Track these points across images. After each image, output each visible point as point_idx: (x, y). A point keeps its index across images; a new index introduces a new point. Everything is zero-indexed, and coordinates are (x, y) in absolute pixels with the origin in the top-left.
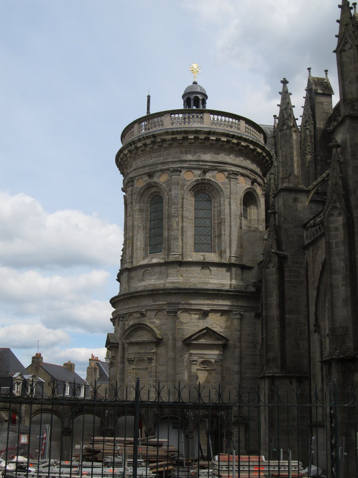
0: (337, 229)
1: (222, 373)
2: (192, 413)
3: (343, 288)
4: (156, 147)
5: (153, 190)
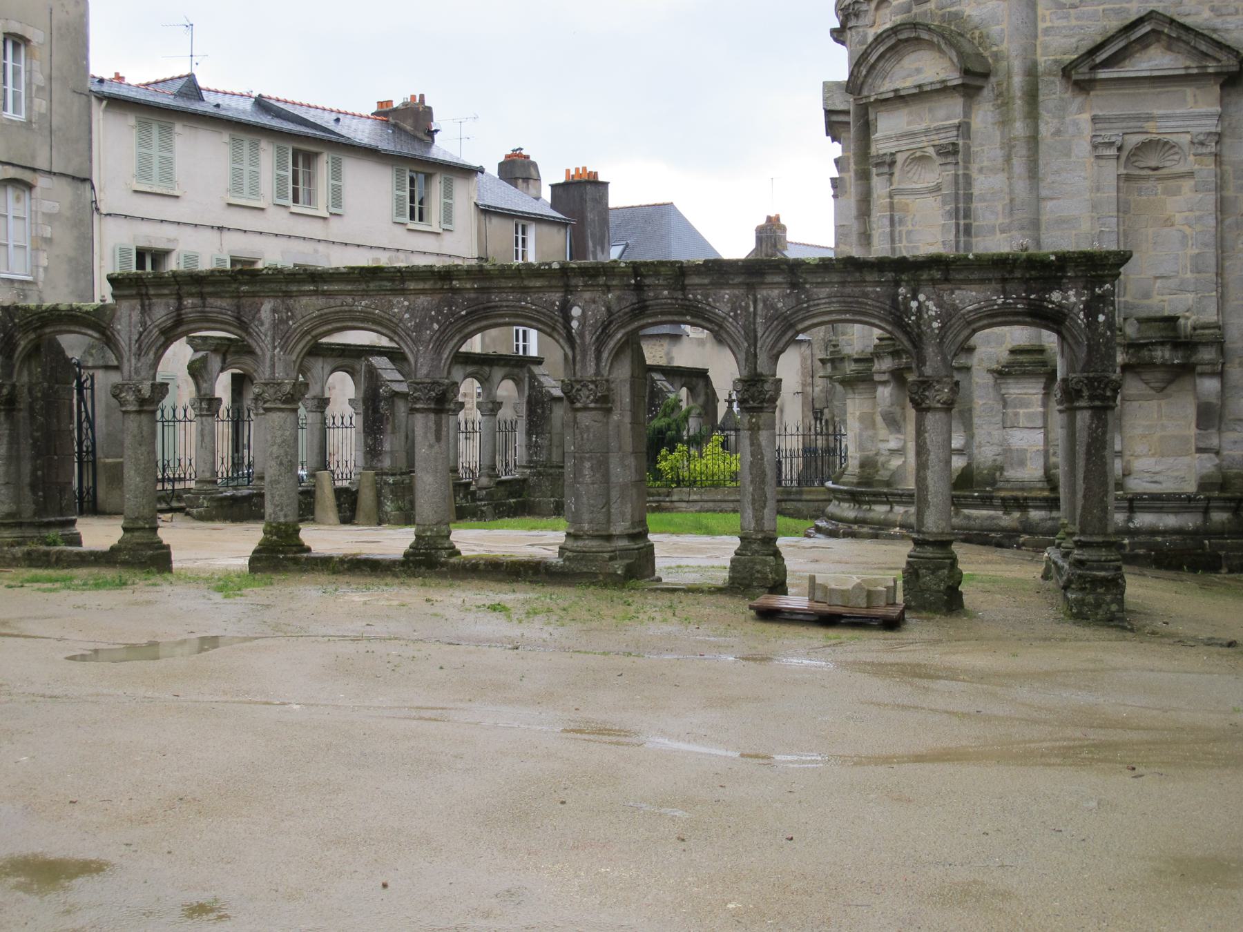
1: (1220, 187)
2: (930, 304)
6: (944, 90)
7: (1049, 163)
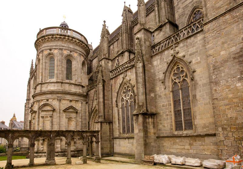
0: (139, 68)
3: (142, 89)
4: (53, 39)
5: (51, 56)
6: (51, 110)
7: (61, 119)
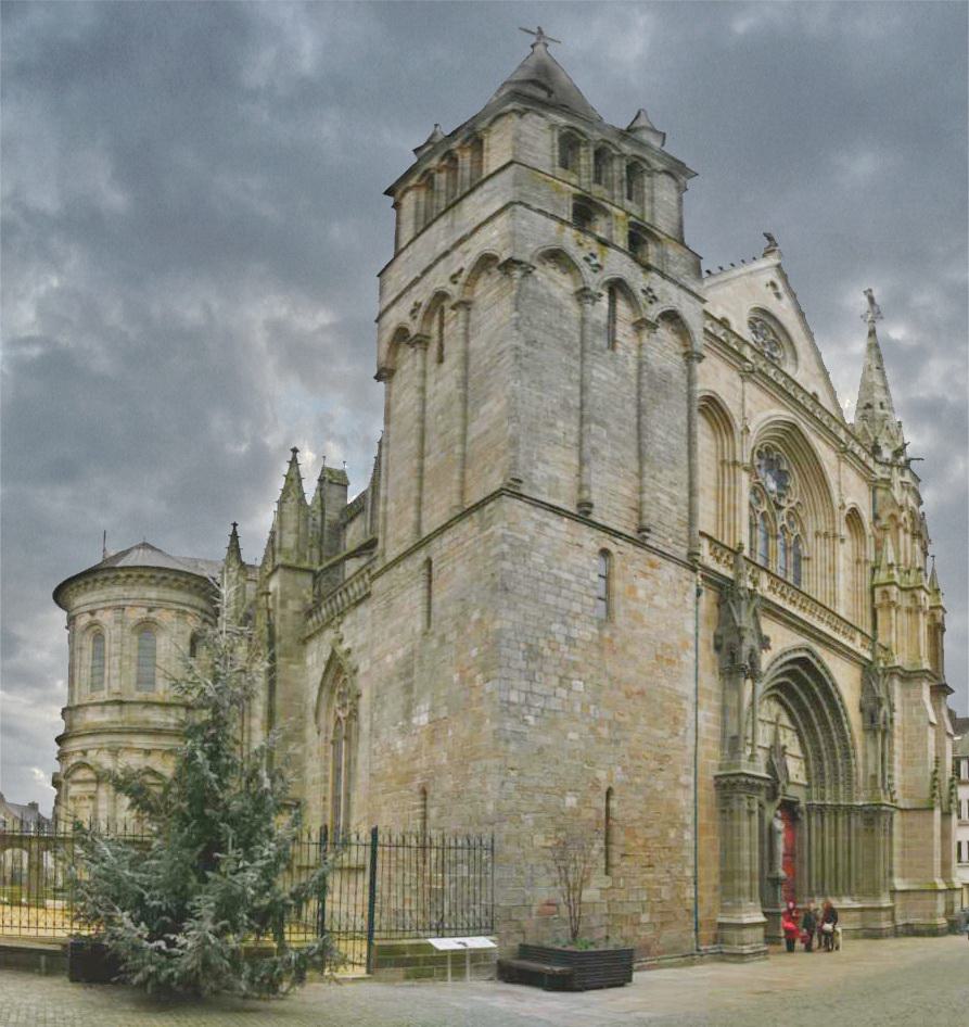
5: (96, 628)
